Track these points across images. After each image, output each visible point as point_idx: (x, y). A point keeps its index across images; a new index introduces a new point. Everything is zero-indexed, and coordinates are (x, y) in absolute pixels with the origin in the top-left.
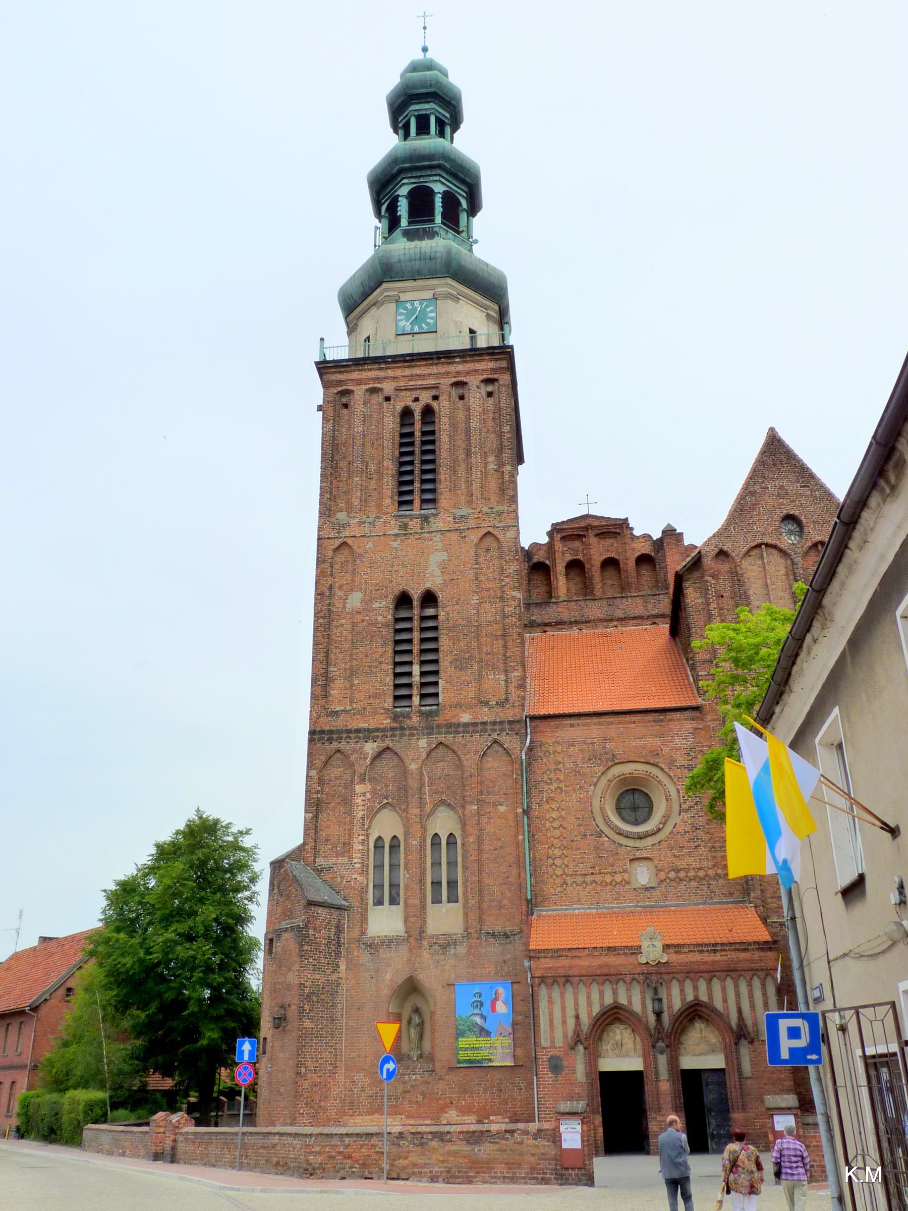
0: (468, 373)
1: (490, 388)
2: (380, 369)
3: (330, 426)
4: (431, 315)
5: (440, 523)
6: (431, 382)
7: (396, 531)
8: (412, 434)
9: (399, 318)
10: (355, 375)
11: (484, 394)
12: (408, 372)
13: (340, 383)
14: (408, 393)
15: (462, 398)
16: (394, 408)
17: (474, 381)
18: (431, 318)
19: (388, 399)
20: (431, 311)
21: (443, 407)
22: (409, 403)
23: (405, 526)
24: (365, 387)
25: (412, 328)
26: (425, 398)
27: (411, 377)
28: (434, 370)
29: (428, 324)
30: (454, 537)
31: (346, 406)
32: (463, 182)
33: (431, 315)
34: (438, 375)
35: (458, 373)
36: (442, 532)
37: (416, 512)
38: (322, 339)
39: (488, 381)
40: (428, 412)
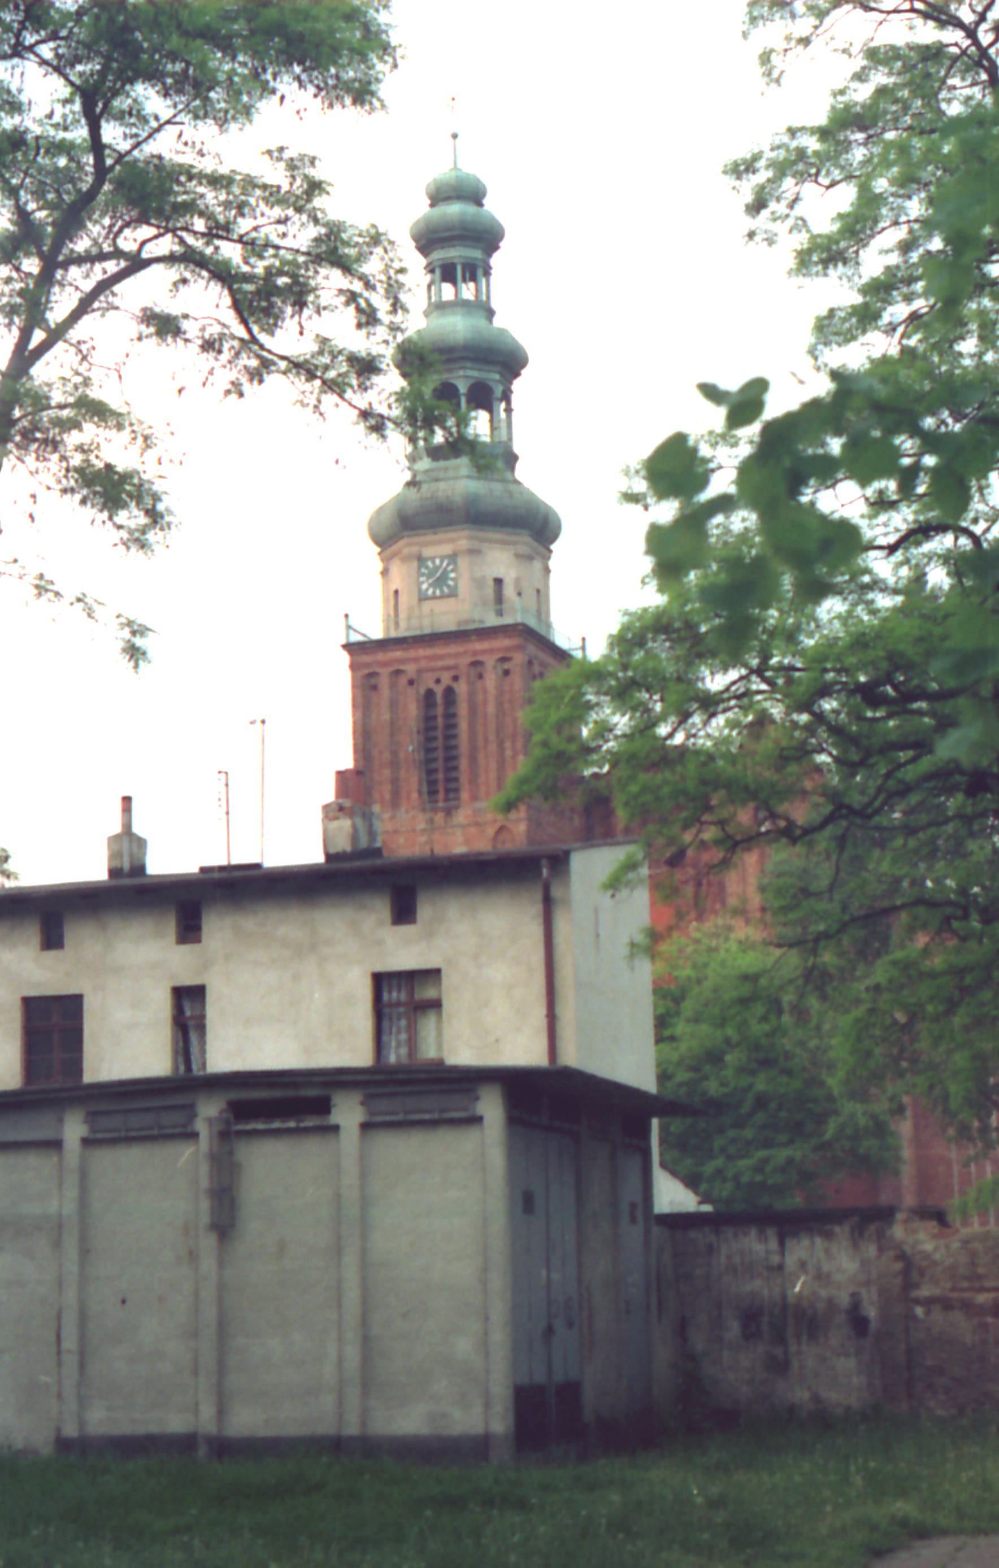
0: (483, 652)
1: (506, 666)
2: (403, 649)
3: (359, 714)
4: (452, 575)
5: (461, 816)
6: (450, 662)
7: (421, 826)
8: (435, 718)
9: (422, 579)
10: (380, 656)
11: (500, 672)
12: (429, 652)
13: (367, 665)
14: (430, 674)
15: (480, 676)
16: (418, 691)
17: (490, 661)
18: (452, 579)
19: (411, 682)
20: (452, 571)
21: (462, 688)
22: (432, 685)
23: (431, 821)
24: (391, 669)
25: (434, 592)
26: (446, 678)
27: (430, 658)
28: (453, 649)
29: (448, 586)
30: (473, 830)
31: (374, 688)
32: (492, 363)
33: (452, 575)
34: (457, 655)
35: (475, 653)
36: (462, 826)
37: (441, 804)
38: (346, 616)
39: (503, 660)
40: (449, 692)
